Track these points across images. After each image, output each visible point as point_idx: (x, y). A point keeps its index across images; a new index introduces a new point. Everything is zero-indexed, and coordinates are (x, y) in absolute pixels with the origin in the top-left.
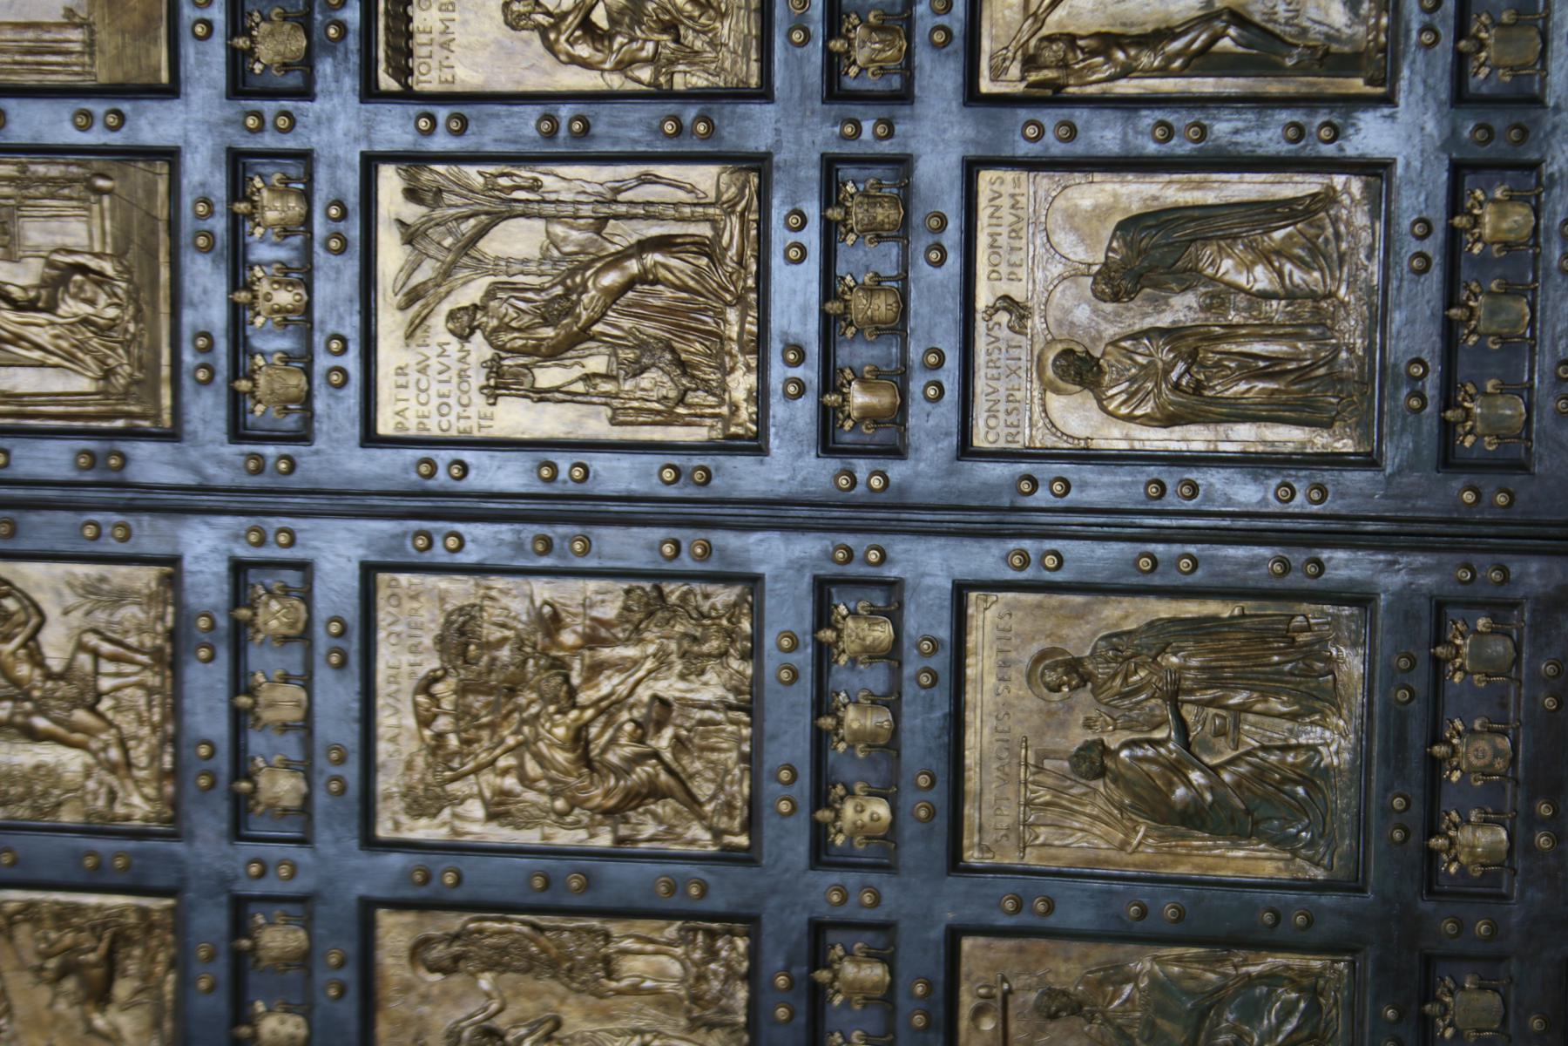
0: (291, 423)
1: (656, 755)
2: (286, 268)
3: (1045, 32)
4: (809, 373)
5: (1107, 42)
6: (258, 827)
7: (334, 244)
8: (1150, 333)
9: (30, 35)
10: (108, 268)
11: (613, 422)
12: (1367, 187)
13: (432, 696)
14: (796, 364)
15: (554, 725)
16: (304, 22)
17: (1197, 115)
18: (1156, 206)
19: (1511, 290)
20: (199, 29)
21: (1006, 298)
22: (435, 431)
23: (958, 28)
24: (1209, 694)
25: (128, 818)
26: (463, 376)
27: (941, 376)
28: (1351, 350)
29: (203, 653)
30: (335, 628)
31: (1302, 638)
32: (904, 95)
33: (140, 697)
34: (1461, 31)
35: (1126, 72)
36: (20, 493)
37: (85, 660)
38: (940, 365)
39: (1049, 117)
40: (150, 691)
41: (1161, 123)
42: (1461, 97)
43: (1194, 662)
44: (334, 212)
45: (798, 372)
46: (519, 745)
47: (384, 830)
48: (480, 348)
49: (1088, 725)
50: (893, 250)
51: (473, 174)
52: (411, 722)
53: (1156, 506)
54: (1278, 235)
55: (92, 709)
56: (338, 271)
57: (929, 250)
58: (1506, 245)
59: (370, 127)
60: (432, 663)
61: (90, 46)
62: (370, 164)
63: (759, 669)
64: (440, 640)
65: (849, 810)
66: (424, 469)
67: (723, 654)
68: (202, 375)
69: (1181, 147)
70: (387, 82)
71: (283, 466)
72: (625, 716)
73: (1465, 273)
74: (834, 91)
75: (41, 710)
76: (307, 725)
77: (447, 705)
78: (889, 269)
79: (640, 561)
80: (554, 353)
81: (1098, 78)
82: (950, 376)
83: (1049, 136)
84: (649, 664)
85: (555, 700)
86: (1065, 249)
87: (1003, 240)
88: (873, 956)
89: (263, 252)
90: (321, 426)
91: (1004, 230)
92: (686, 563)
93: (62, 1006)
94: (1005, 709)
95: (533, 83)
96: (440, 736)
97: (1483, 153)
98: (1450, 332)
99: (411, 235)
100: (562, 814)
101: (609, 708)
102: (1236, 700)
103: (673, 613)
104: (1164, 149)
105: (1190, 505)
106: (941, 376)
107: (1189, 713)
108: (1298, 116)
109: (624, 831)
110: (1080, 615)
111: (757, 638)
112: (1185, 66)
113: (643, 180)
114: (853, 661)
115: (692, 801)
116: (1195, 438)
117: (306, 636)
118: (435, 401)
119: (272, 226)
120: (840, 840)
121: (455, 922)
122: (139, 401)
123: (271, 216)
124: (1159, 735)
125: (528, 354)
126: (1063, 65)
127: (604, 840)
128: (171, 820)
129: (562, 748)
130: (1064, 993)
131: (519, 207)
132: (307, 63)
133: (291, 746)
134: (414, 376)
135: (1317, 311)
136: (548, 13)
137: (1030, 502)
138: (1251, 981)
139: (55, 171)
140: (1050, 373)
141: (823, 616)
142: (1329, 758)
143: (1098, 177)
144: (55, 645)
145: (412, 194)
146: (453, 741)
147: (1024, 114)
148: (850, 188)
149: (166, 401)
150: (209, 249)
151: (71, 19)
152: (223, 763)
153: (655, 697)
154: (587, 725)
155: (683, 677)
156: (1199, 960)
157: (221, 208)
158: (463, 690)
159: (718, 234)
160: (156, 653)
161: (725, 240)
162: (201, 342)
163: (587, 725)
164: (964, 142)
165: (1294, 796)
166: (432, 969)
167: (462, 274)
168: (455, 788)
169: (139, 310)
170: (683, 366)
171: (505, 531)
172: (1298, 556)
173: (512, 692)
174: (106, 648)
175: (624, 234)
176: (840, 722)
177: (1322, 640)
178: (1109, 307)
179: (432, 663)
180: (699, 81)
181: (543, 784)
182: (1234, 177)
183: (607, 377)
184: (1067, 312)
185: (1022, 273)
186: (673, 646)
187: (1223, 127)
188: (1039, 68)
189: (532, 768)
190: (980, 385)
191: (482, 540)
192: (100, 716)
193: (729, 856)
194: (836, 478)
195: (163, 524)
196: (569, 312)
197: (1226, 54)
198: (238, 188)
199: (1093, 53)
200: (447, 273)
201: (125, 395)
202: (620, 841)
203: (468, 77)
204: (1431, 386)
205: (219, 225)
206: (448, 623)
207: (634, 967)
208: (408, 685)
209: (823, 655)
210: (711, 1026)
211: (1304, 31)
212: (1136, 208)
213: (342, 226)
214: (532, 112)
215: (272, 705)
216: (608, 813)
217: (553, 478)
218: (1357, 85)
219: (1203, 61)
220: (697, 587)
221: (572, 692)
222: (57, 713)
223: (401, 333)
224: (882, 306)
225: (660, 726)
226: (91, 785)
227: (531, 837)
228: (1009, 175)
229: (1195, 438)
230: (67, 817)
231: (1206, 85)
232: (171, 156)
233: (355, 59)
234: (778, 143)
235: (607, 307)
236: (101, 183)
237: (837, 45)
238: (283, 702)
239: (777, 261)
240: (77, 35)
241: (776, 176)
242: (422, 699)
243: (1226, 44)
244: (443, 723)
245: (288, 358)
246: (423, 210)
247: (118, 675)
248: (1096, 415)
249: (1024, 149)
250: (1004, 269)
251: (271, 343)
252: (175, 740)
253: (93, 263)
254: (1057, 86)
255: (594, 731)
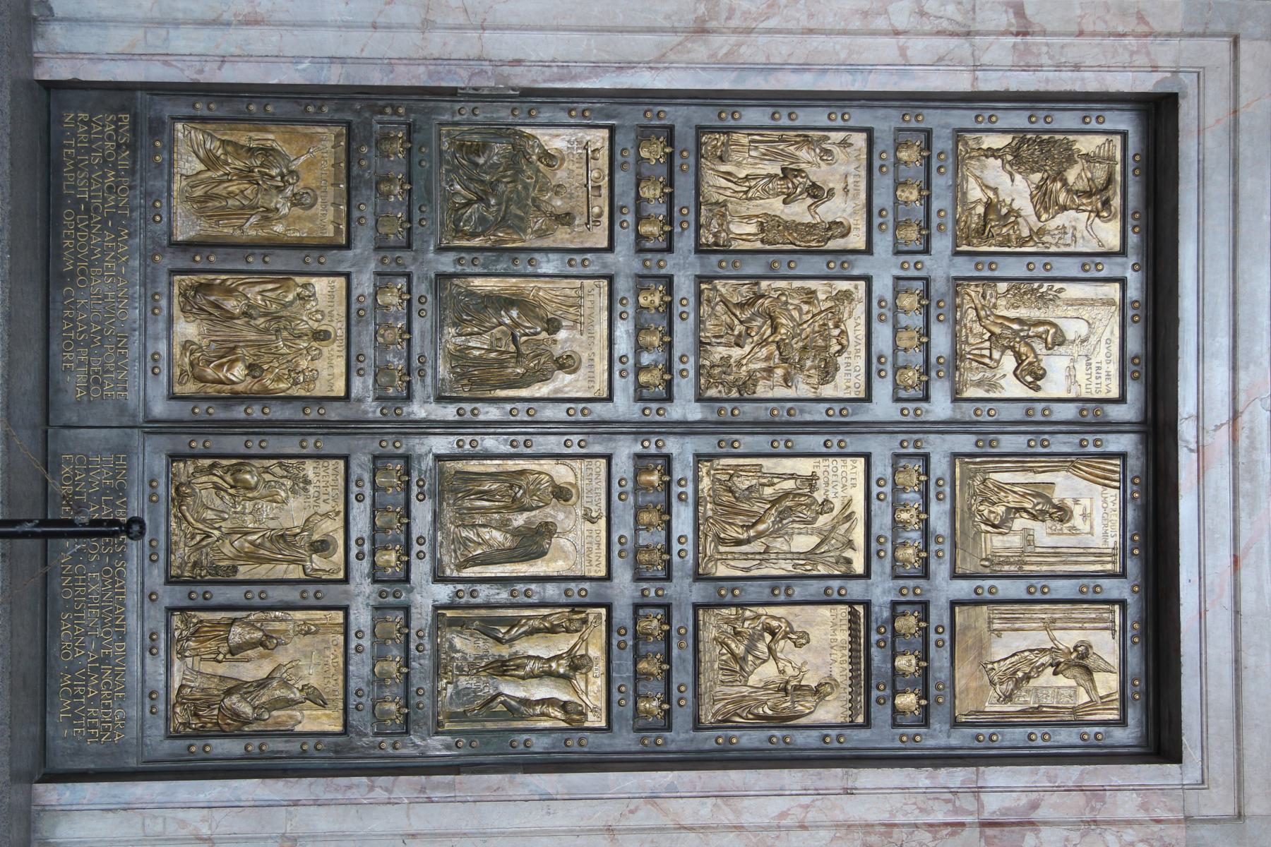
0: (903, 462)
1: (741, 322)
2: (904, 528)
3: (579, 634)
4: (676, 490)
5: (552, 630)
6: (919, 285)
7: (882, 540)
8: (531, 509)
9: (1017, 626)
10: (983, 527)
11: (761, 466)
12: (444, 572)
13: (841, 344)
14: (681, 493)
15: (786, 334)
16: (895, 633)
17: (514, 600)
18: (532, 562)
19: (384, 530)
20: (941, 630)
21: (593, 523)
22: (839, 459)
23: (615, 635)
24: (504, 357)
25: (977, 286)
26: (827, 484)
27: (620, 489)
28: (448, 504)
29: (942, 360)
30: (883, 374)
31: (465, 382)
32: (637, 607)
33: (971, 340)
34: (408, 635)
35: (545, 617)
36: (1023, 428)
37: (996, 355)
38: (620, 494)
39: (576, 598)
40: (967, 342)
41: (529, 597)
42: (406, 609)
43: (510, 370)
44: (882, 554)
45: (681, 489)
46: (801, 325)
47: (862, 284)
48: (819, 496)
49: (555, 341)
50: (641, 542)
51: (822, 570)
52: (850, 334)
53: (528, 437)
54: (479, 551)
55: (993, 334)
56: (881, 528)
57: (626, 543)
58: (386, 549)
59: (867, 590)
60: (841, 360)
61: (990, 622)
62: (867, 574)
63: (697, 361)
64: (837, 369)
65: (657, 302)
66: (843, 444)
67: (712, 367)
68: (941, 482)
69: (521, 587)
70: (860, 609)
71: (905, 444)
72: (755, 338)
73: (402, 538)
74: (667, 607)
75: (1016, 333)
76: (896, 330)
77: (834, 341)
78: (643, 534)
79: (747, 407)
80: (786, 494)
81: (557, 616)
82: (616, 489)
83: (576, 591)
84: (744, 362)
85: (786, 345)
86: (568, 544)
87: (595, 547)
88: (647, 238)
89: (915, 536)
90: (888, 462)
91: (594, 551)
92: (728, 406)
93: (1008, 201)
94: (590, 345)
95: (797, 609)
96: (837, 326)
97: (397, 587)
98: (408, 513)
99: (850, 544)
100: (783, 294)
101: (763, 343)
102: (493, 355)
103: (734, 384)
104: (528, 586)
105: (513, 437)
106: (620, 489)
107: (512, 348)
108: (473, 601)
109: (756, 288)
110: (556, 391)
111: (698, 374)
112: (520, 621)
113: (748, 569)
114: (656, 366)
115: (725, 302)
116: (512, 465)
117: (896, 369)
118: (839, 472)
119: (910, 546)
120: (661, 288)
121: (831, 245)
122: (970, 470)
123: (910, 551)
124: (524, 338)
125: (798, 494)
126: (570, 620)
127: (764, 284)
128: (957, 285)
129: (783, 324)
130: (563, 225)
131: (802, 556)
132: (894, 617)
133: (903, 320)
134: (849, 484)
135: (463, 520)
136: (790, 639)
137: (581, 437)
138: (482, 233)
139: (1006, 568)
140: (574, 491)
141: (669, 385)
142: (453, 331)
143: (555, 574)
144: (1009, 362)
145: (849, 561)
146: (831, 324)
147: (587, 600)
148: (660, 568)
149: (958, 470)
150: (938, 537)
151: (999, 633)
152: (933, 312)
153: (742, 347)
154: (772, 334)
155: (730, 357)
156: (506, 242)
157: (932, 554)
158: (827, 348)
159: (716, 546)
160: (963, 359)
161: (713, 545)
162: (941, 496)
163: (772, 334)
164: (612, 588)
165: (468, 315)
166: (841, 223)
167: (828, 527)
168: (830, 304)
169: (970, 509)
170: (731, 491)
171: (808, 418)
172: (468, 416)
173: (804, 348)
174: (987, 361)
175: (757, 546)
176: (661, 339)
177: (457, 381)
178: (550, 520)
179: (841, 360)
180: (725, 611)
181: (791, 307)
182: (498, 575)
183: (764, 485)
184: (566, 517)
185: (586, 533)
186: (734, 369)
187: (503, 595)
188: (581, 619)
189: (795, 314)
190: (603, 484)
191: (817, 413)
192: (989, 331)
193: (709, 279)
194: (664, 445)
195: (958, 417)
196: (780, 513)
197: (504, 626)
198: (926, 563)
199: (558, 625)
200: (834, 528)
201: (977, 471)
202: (757, 284)
203: (825, 611)
204: (415, 489)
205: (933, 547)
206: (833, 377)
207: (752, 229)
208: (851, 349)
209: (669, 368)
210: (717, 203)
211: (471, 636)
212: (539, 561)
213: (879, 548)
214: (796, 597)
215: (912, 338)
216: (762, 296)
217: (787, 441)
218: (449, 613)
219: (513, 623)
220: (724, 395)
221: (778, 348)
222: (1008, 332)
223: (854, 502)
224: (645, 517)
225: (740, 335)
226: (993, 300)
227: (797, 284)
228: (593, 574)
229: (512, 465)
230: (1002, 287)
231: (510, 613)
232: (955, 576)
233: (873, 618)
234: (690, 586)
235: (764, 515)
236: (987, 563)
237: (666, 627)
238: (905, 340)
239: (691, 537)
240: (996, 626)
241: (691, 573)
242: (844, 342)
243: (503, 631)
244: (836, 332)
245: (904, 490)
246: (844, 555)
247: (981, 349)
248: (553, 473)
249: (586, 585)
250: (594, 535)
251: (912, 497)
252: (956, 322)
253: (989, 529)
254: (573, 612)
255: (769, 332)
